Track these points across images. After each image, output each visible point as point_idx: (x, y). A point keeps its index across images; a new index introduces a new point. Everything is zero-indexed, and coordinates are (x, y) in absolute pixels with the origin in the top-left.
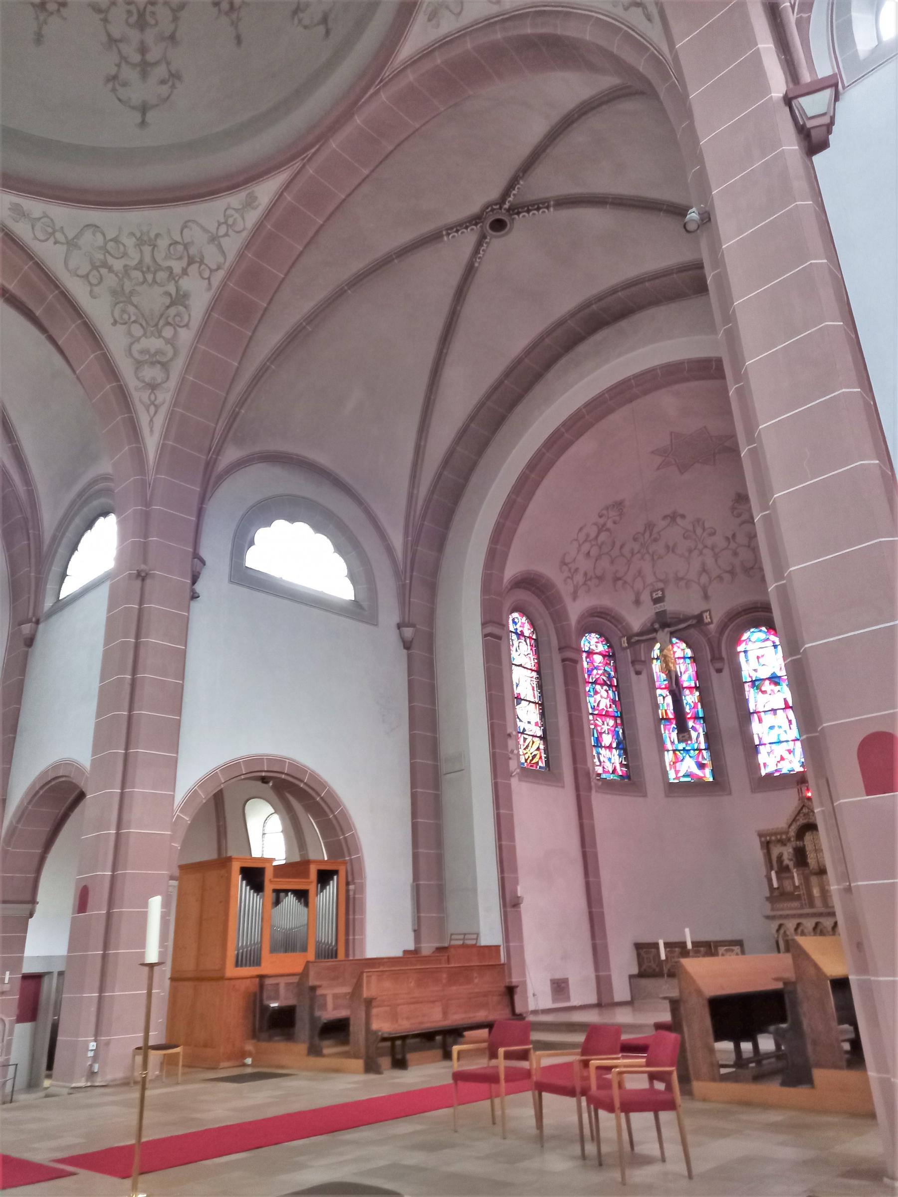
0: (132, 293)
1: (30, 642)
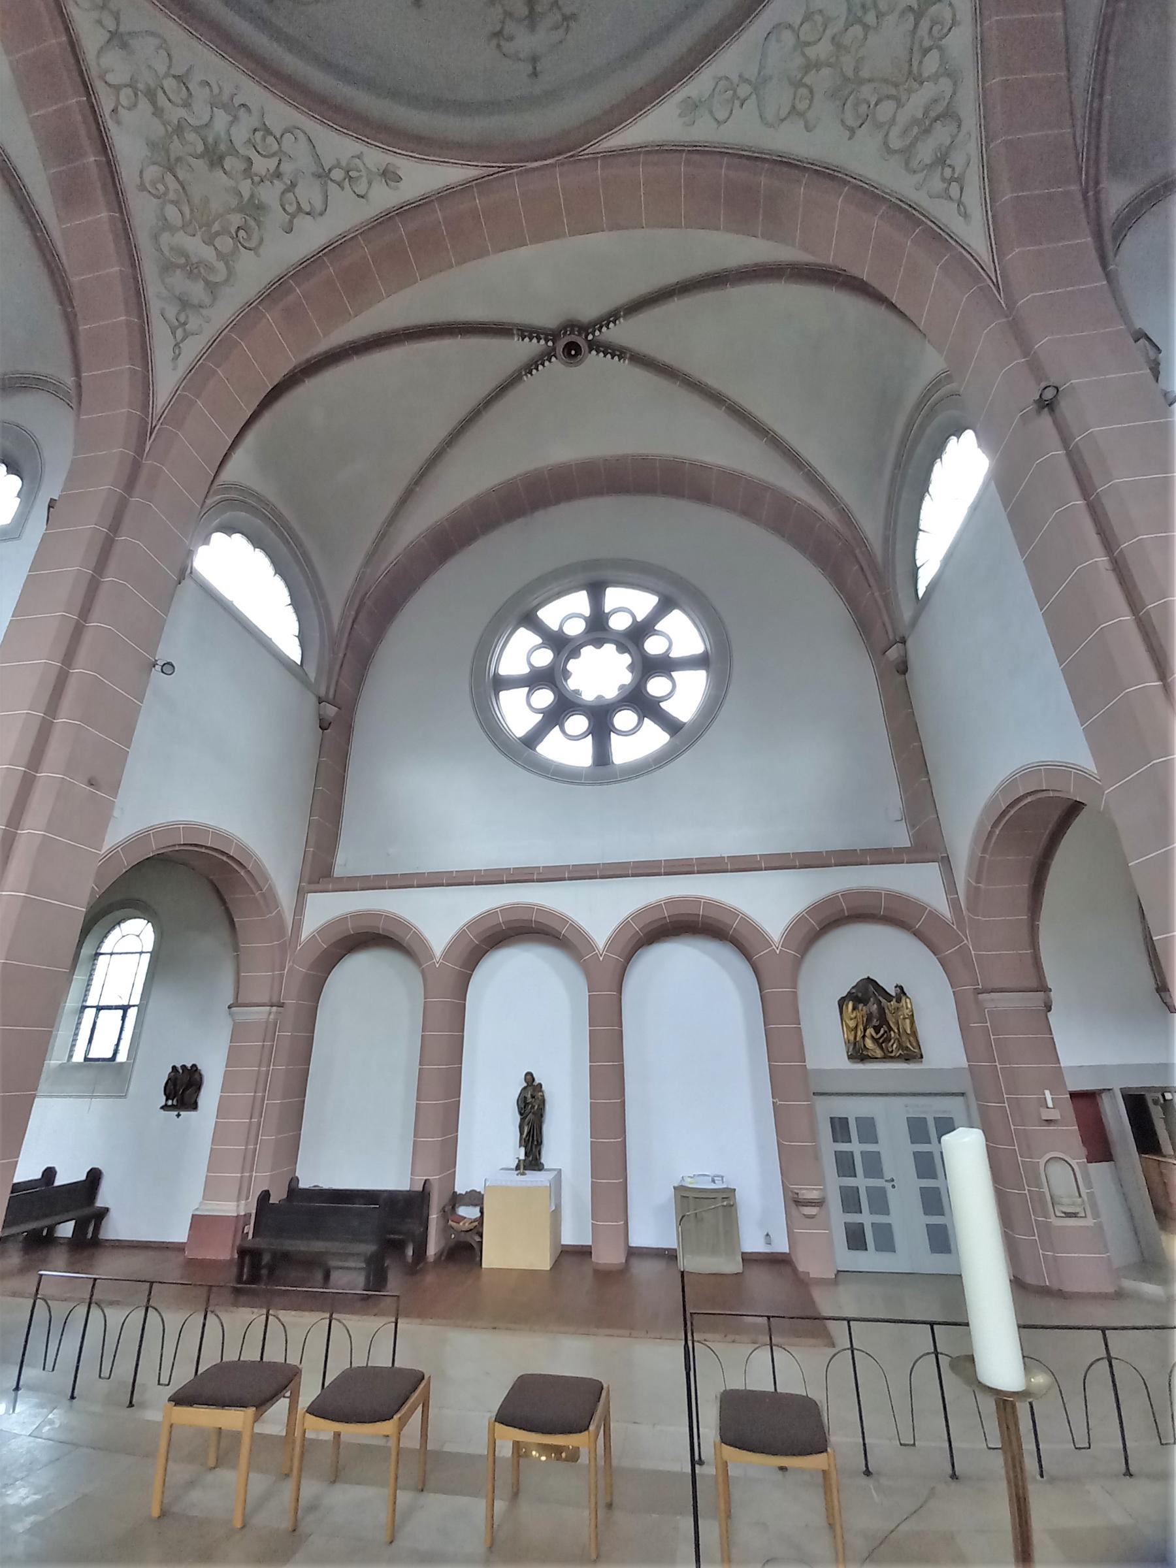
0: (857, 70)
1: (903, 668)
